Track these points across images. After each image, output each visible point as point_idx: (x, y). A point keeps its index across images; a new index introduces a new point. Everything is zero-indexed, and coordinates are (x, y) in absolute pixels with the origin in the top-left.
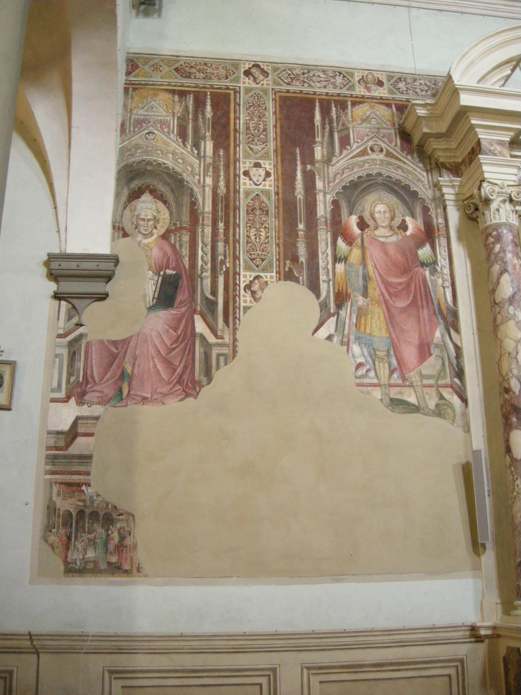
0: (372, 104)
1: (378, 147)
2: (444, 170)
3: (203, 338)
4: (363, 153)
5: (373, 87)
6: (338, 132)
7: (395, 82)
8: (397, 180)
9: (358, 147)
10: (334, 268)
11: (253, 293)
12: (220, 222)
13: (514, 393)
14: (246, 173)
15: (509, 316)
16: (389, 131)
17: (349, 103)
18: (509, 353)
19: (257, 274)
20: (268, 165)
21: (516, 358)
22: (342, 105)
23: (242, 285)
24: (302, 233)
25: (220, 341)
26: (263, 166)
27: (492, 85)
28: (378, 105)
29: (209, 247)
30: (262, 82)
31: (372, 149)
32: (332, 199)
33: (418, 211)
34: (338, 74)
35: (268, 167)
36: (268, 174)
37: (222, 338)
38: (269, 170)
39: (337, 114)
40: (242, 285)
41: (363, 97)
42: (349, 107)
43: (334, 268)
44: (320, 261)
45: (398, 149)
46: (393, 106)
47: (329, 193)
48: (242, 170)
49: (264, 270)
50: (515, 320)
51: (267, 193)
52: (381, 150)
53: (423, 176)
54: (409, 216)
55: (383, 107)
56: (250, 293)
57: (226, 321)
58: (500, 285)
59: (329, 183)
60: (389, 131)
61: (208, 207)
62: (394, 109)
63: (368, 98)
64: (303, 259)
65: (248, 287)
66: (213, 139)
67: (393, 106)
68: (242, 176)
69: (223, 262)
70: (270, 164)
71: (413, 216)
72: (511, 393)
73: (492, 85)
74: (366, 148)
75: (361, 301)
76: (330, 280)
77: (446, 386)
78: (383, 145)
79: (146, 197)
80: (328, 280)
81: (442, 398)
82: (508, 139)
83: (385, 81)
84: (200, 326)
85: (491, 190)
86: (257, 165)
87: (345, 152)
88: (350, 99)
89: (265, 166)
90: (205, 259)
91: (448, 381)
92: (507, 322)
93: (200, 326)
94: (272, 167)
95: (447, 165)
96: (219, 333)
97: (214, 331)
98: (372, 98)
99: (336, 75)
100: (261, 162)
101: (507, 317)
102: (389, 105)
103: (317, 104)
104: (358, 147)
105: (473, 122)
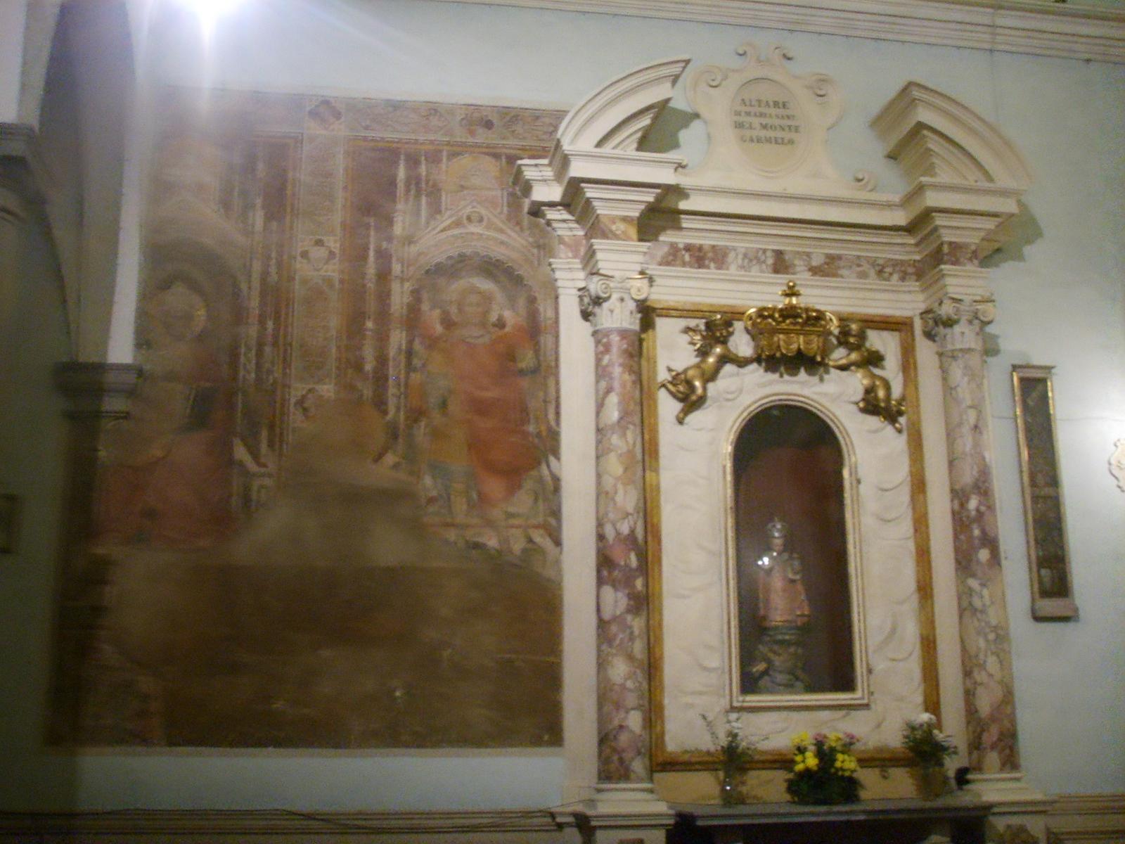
0: (475, 155)
1: (477, 215)
2: (562, 246)
3: (241, 464)
4: (458, 224)
5: (480, 131)
6: (427, 196)
7: (509, 121)
8: (497, 260)
9: (450, 217)
10: (407, 377)
11: (305, 410)
12: (268, 319)
13: (607, 541)
14: (305, 255)
15: (611, 447)
16: (494, 193)
17: (445, 153)
18: (607, 493)
19: (311, 386)
20: (333, 243)
21: (613, 499)
22: (434, 158)
23: (293, 400)
24: (370, 333)
25: (263, 470)
26: (326, 244)
27: (614, 148)
28: (483, 156)
29: (254, 352)
30: (332, 127)
31: (469, 219)
32: (411, 288)
33: (521, 302)
34: (433, 112)
35: (332, 244)
36: (332, 254)
37: (265, 466)
38: (334, 250)
39: (427, 171)
40: (293, 400)
41: (463, 144)
42: (445, 159)
43: (407, 377)
44: (391, 370)
45: (503, 217)
46: (503, 157)
47: (408, 280)
48: (299, 250)
49: (320, 381)
50: (617, 452)
51: (329, 281)
52: (481, 220)
53: (533, 255)
54: (509, 309)
55: (488, 159)
56: (301, 410)
57: (271, 444)
58: (605, 407)
59: (408, 267)
60: (494, 193)
61: (254, 303)
62: (504, 160)
63: (470, 146)
64: (369, 367)
65: (300, 402)
66: (263, 207)
67: (503, 157)
68: (299, 258)
69: (269, 372)
70: (335, 242)
71: (513, 307)
72: (604, 541)
73: (614, 148)
74: (462, 217)
75: (437, 418)
76: (401, 394)
77: (537, 527)
78: (483, 212)
79: (179, 289)
80: (398, 394)
81: (530, 541)
82: (637, 214)
83: (495, 121)
84: (241, 453)
85: (604, 286)
86: (319, 243)
87: (432, 223)
88: (448, 148)
89: (329, 245)
90: (248, 367)
91: (540, 519)
92: (607, 454)
93: (241, 453)
94: (338, 245)
95: (566, 239)
96: (263, 460)
97: (255, 455)
98: (476, 145)
99: (431, 114)
100: (325, 239)
101: (609, 448)
102: (496, 156)
103: (402, 157)
104: (450, 217)
105: (588, 195)
